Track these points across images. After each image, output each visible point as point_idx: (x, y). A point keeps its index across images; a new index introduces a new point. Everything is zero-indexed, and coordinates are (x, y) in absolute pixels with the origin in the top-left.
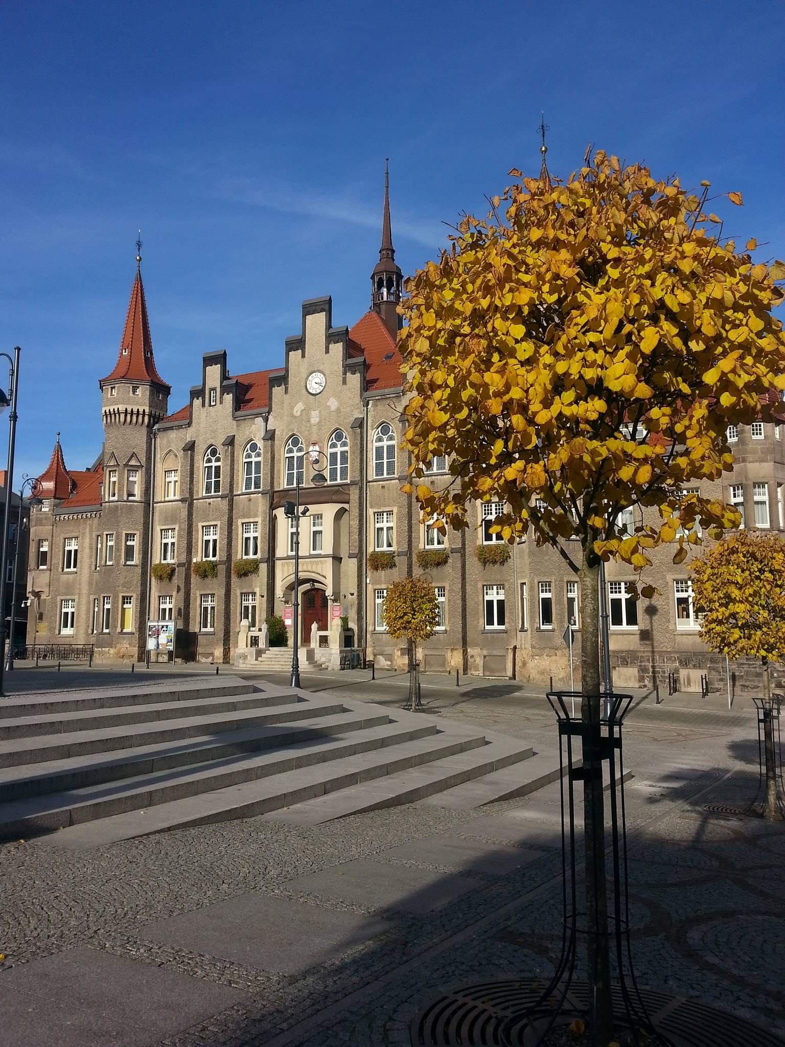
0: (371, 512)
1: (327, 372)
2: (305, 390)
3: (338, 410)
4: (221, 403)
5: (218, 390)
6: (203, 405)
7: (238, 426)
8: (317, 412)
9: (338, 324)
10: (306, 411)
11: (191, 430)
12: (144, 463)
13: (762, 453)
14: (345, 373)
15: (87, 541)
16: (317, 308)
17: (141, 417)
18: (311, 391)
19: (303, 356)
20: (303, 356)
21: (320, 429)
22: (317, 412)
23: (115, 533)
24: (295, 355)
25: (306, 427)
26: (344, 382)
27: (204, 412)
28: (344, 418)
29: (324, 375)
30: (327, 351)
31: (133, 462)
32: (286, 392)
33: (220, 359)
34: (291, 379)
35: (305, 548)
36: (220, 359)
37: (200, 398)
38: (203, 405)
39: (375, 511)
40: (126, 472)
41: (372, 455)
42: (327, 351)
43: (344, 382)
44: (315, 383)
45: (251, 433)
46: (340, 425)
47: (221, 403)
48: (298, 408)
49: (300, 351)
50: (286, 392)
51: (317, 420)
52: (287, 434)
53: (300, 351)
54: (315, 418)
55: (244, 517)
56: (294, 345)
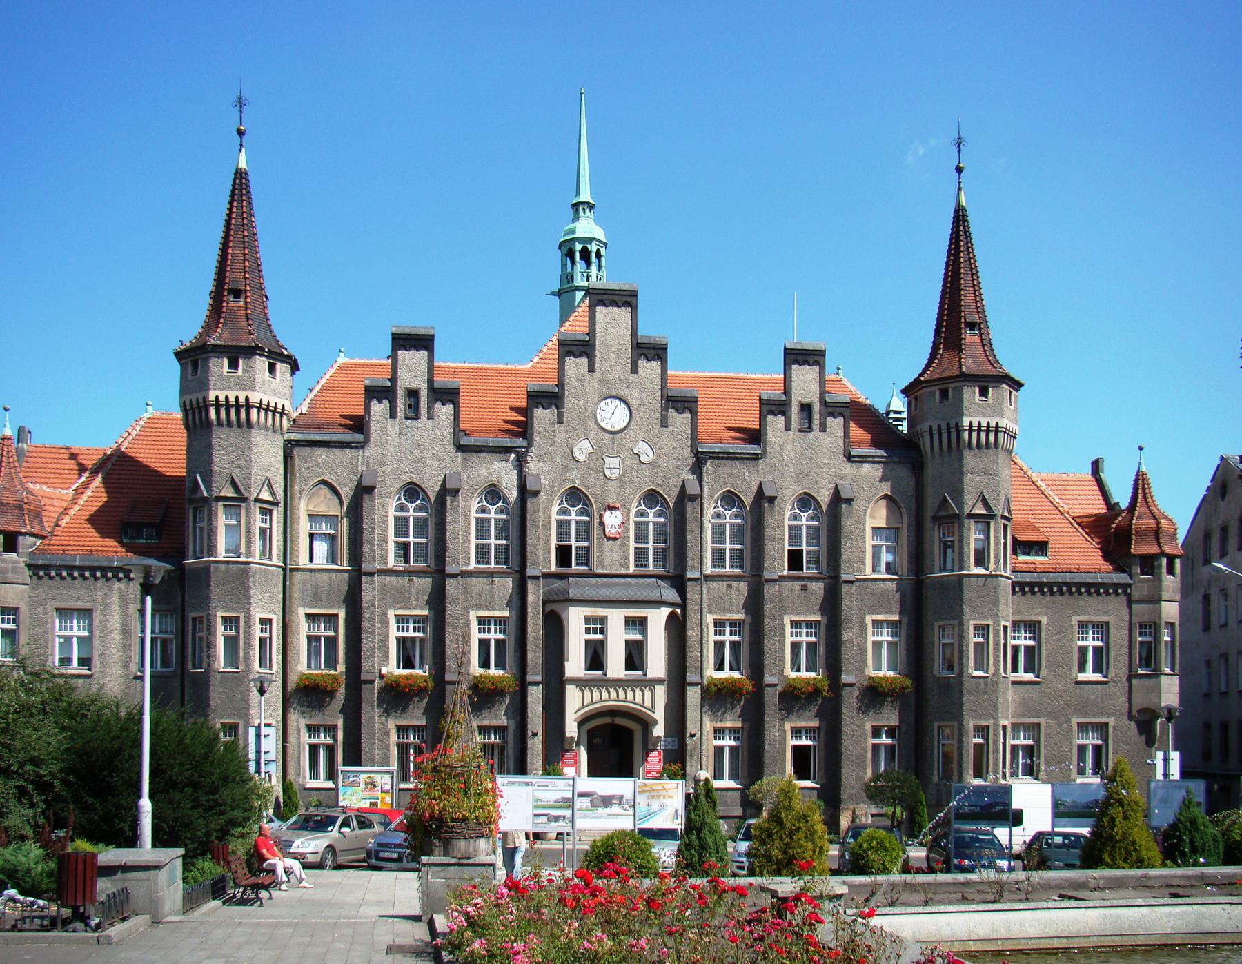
0: (709, 619)
1: (634, 402)
2: (592, 424)
3: (653, 465)
4: (430, 416)
5: (424, 394)
6: (393, 415)
7: (465, 459)
8: (617, 460)
9: (647, 331)
10: (598, 456)
11: (368, 452)
12: (281, 498)
13: (1173, 591)
14: (665, 409)
15: (115, 620)
16: (616, 298)
17: (278, 415)
18: (603, 425)
19: (591, 369)
20: (591, 369)
21: (621, 487)
22: (617, 460)
23: (242, 616)
24: (576, 366)
25: (598, 479)
26: (664, 424)
27: (393, 427)
28: (664, 477)
29: (628, 406)
30: (634, 370)
31: (265, 495)
32: (560, 421)
33: (423, 342)
34: (569, 401)
35: (616, 665)
36: (423, 342)
37: (386, 402)
38: (393, 415)
39: (716, 617)
40: (258, 510)
41: (708, 536)
42: (634, 370)
43: (664, 424)
44: (613, 415)
45: (491, 474)
46: (658, 485)
47: (430, 416)
48: (582, 449)
49: (585, 360)
50: (560, 421)
51: (616, 473)
52: (561, 486)
53: (584, 361)
54: (613, 465)
55: (479, 607)
56: (574, 349)
